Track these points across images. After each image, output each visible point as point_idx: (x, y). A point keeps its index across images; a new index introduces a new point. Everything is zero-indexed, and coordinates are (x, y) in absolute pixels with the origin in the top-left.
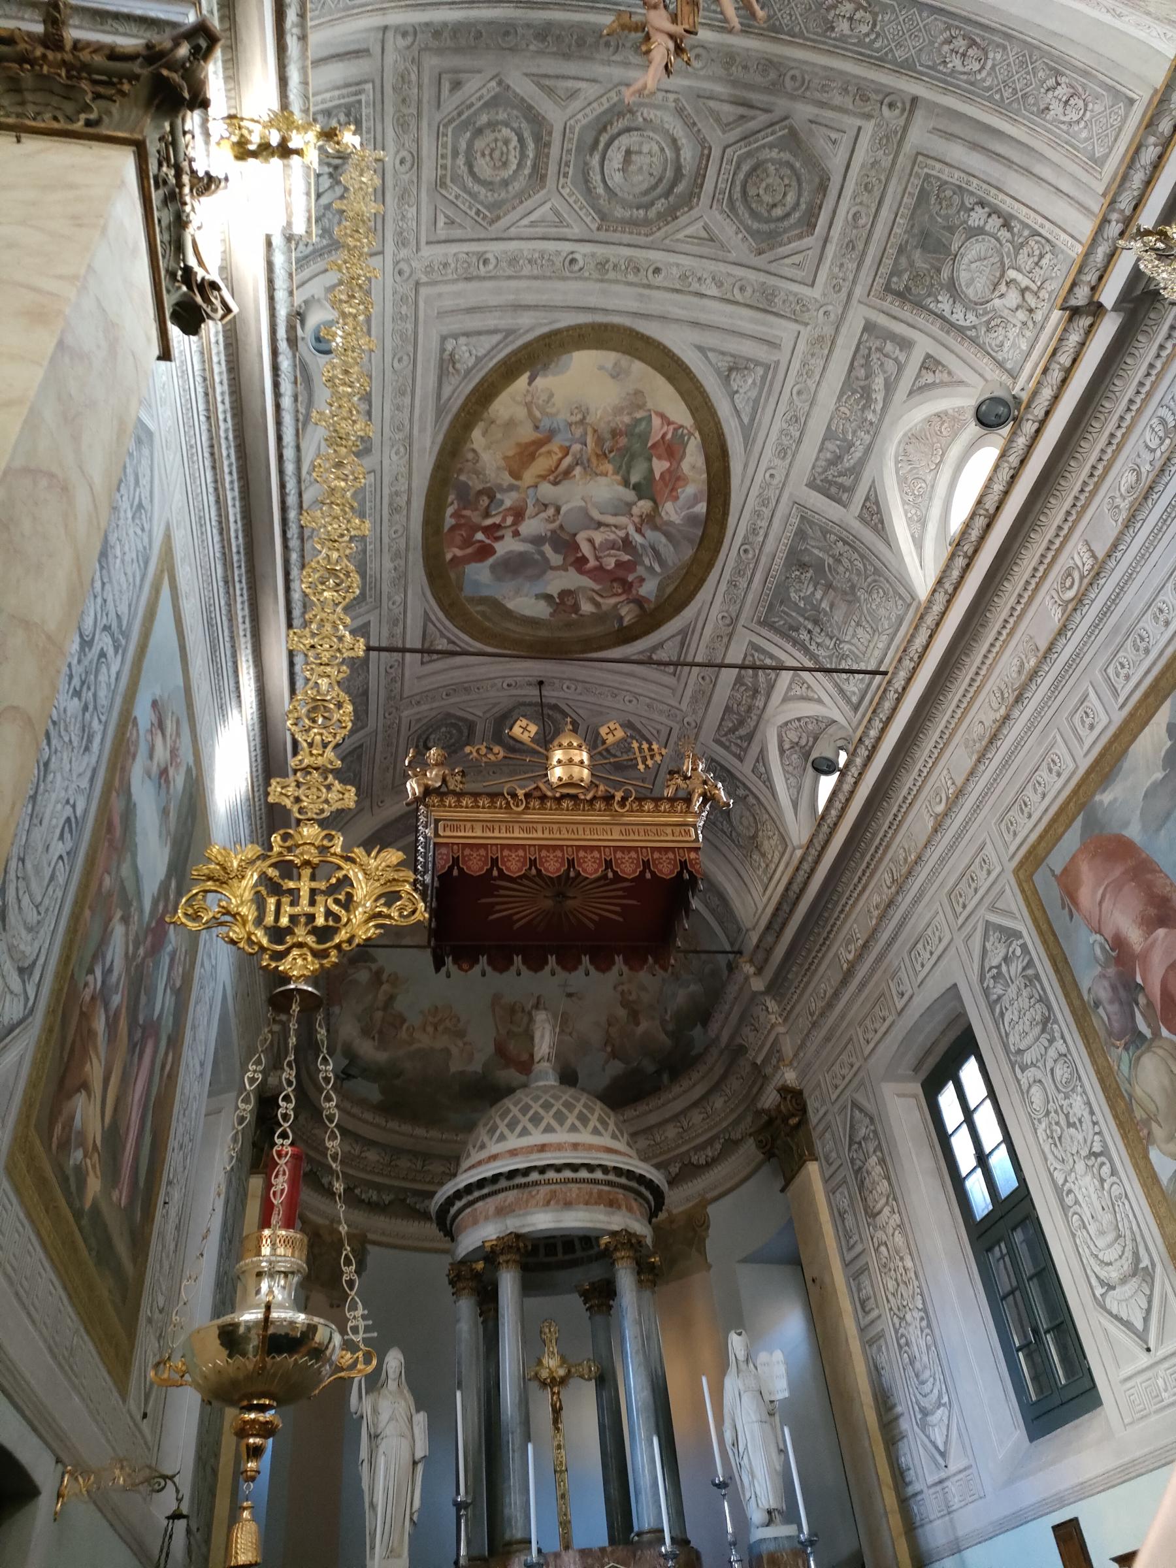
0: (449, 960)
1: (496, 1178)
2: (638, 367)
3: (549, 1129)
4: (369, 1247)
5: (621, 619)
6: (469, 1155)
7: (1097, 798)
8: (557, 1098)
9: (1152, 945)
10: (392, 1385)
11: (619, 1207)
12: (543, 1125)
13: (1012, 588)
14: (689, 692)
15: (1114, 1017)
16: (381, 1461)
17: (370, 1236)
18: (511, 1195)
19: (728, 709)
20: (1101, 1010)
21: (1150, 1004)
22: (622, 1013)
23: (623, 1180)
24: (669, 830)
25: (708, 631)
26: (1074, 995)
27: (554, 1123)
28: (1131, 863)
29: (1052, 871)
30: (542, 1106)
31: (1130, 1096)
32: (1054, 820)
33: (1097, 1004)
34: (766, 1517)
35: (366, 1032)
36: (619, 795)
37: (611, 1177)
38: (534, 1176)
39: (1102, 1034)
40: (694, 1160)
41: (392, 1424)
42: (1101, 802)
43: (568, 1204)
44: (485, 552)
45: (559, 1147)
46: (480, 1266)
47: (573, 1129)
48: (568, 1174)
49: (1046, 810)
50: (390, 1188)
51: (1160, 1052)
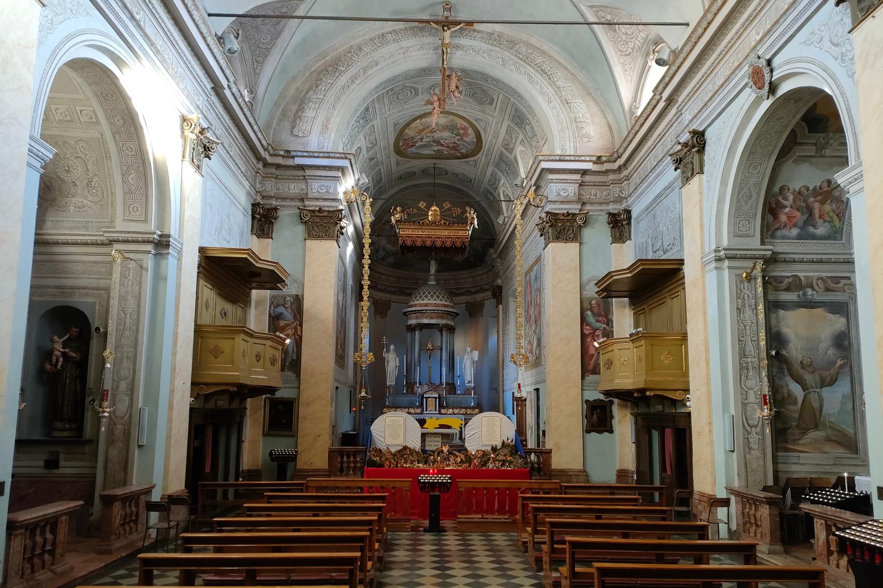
1: (415, 311)
2: (450, 116)
3: (429, 299)
10: (392, 352)
16: (389, 365)
25: (482, 162)
35: (389, 243)
36: (448, 223)
43: (432, 318)
44: (412, 146)
45: (431, 305)
47: (435, 300)
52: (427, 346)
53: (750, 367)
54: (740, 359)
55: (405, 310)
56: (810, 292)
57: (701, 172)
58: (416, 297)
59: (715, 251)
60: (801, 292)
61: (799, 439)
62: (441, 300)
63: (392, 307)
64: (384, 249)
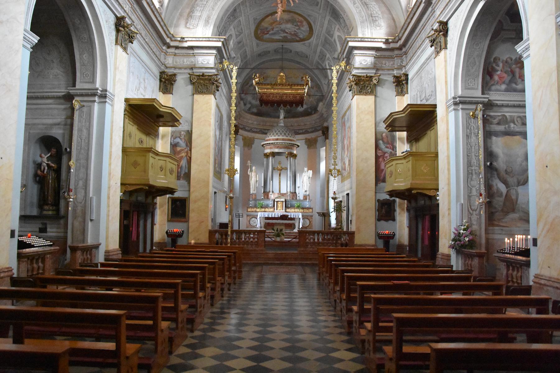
0: (263, 104)
3: (279, 136)
45: (280, 140)
47: (283, 136)
53: (474, 173)
54: (468, 167)
55: (263, 143)
56: (512, 125)
57: (446, 48)
58: (270, 134)
59: (454, 98)
60: (507, 126)
61: (502, 219)
62: (287, 136)
63: (255, 142)
64: (250, 103)
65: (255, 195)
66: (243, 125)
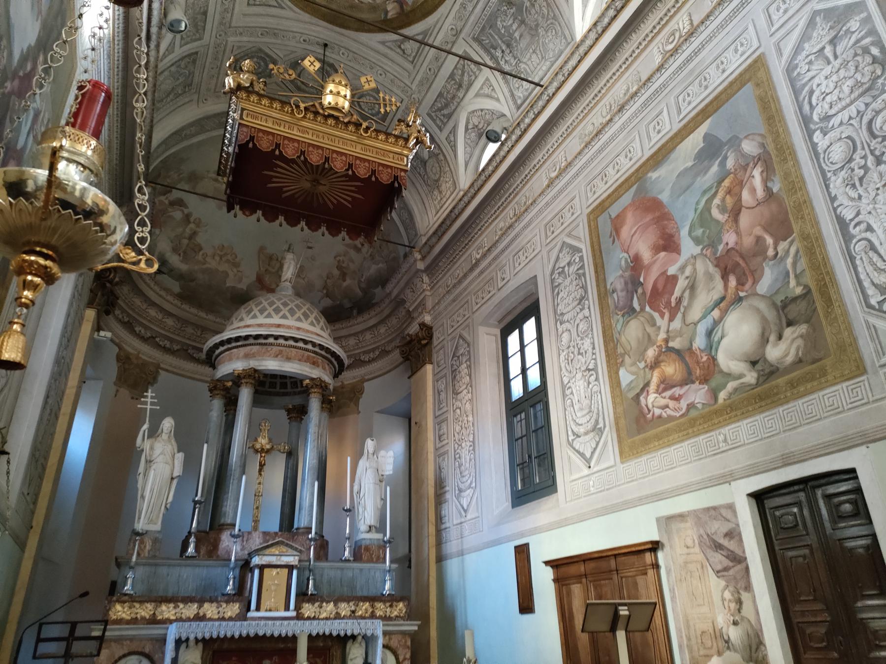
0: (237, 207)
1: (247, 337)
3: (284, 317)
4: (160, 371)
5: (386, 12)
6: (232, 323)
7: (649, 175)
8: (293, 301)
9: (654, 262)
10: (165, 436)
11: (318, 366)
12: (281, 314)
13: (636, 38)
14: (419, 77)
15: (621, 299)
16: (152, 473)
17: (162, 365)
18: (255, 349)
19: (440, 95)
20: (615, 295)
21: (644, 293)
22: (336, 272)
23: (323, 353)
24: (391, 155)
26: (602, 285)
27: (288, 314)
28: (657, 214)
29: (610, 215)
30: (282, 304)
31: (618, 341)
32: (620, 186)
33: (613, 292)
34: (368, 528)
36: (365, 125)
37: (317, 349)
38: (271, 340)
39: (612, 307)
40: (362, 358)
41: (161, 457)
42: (651, 178)
43: (288, 359)
45: (289, 327)
46: (229, 384)
47: (299, 319)
48: (292, 343)
49: (617, 180)
50: (178, 342)
51: (642, 319)
52: (256, 440)
63: (160, 378)
65: (155, 541)
66: (129, 315)
